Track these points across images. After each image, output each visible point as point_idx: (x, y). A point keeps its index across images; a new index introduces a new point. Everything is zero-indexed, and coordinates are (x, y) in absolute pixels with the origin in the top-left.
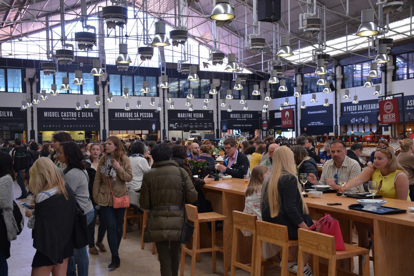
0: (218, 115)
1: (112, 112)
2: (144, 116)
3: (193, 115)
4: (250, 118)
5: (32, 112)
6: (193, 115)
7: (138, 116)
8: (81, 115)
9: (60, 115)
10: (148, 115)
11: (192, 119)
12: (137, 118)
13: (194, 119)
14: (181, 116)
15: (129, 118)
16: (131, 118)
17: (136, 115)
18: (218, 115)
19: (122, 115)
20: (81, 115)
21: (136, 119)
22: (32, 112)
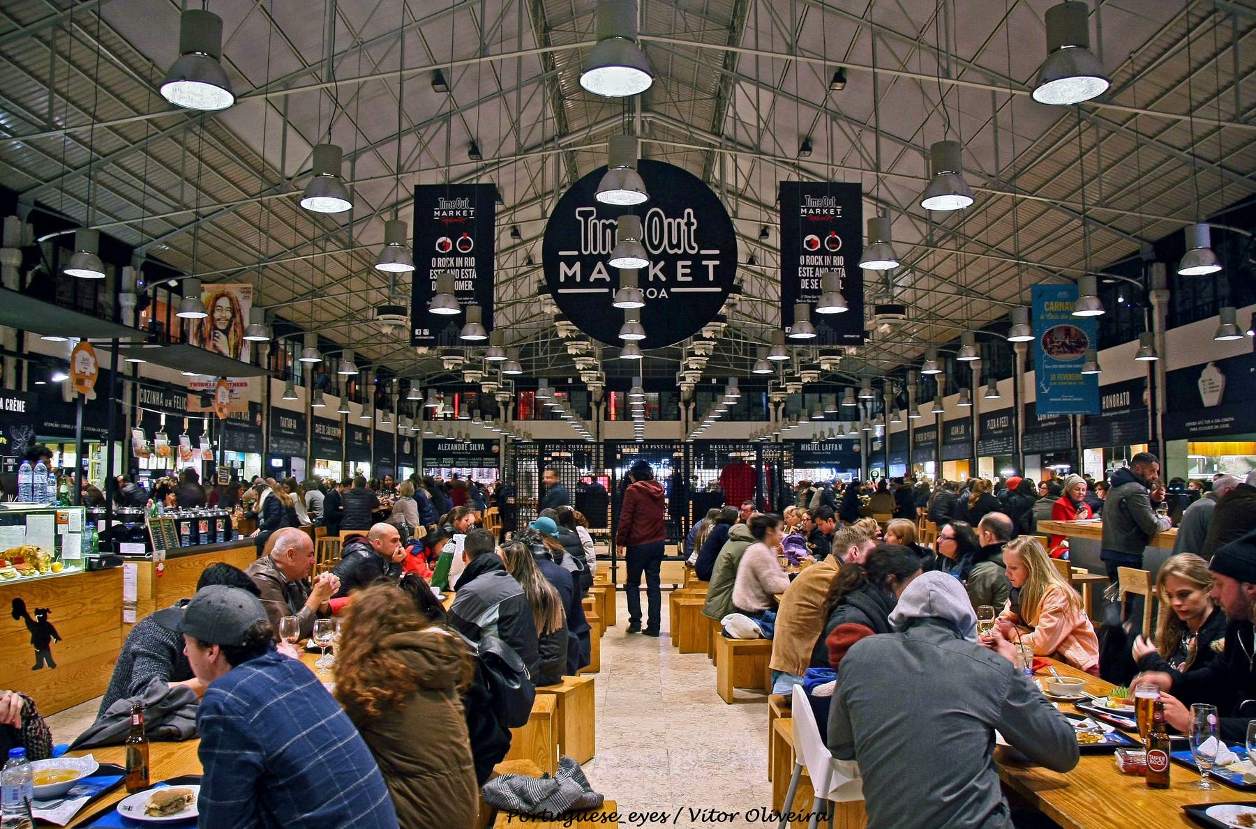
4: (838, 451)
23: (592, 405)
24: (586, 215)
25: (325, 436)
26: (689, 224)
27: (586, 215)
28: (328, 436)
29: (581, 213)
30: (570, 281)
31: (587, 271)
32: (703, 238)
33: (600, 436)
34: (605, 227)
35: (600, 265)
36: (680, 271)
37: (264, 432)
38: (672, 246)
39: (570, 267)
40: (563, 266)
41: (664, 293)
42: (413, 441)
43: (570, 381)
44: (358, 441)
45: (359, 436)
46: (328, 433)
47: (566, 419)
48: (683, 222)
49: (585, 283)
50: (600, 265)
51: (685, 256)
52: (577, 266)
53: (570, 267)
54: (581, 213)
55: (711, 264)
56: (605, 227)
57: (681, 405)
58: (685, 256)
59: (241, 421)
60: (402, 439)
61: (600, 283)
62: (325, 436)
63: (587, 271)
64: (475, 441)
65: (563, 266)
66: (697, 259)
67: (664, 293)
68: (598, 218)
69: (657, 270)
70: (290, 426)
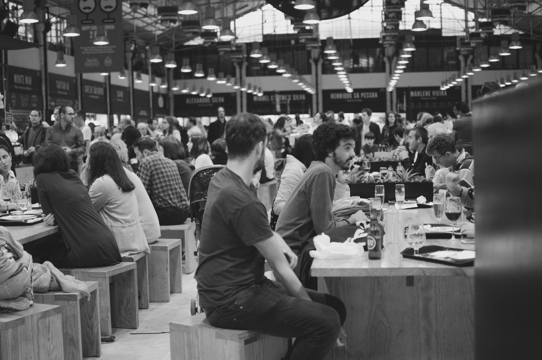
0: (467, 91)
1: (327, 93)
2: (366, 96)
3: (431, 94)
5: (241, 97)
6: (431, 94)
7: (358, 96)
8: (292, 98)
9: (270, 98)
10: (372, 95)
11: (430, 99)
12: (357, 99)
13: (433, 98)
14: (416, 95)
15: (347, 99)
16: (350, 99)
17: (356, 95)
18: (467, 91)
19: (339, 96)
20: (292, 98)
21: (356, 101)
22: (241, 97)
23: (311, 61)
25: (93, 94)
28: (95, 95)
33: (319, 87)
37: (44, 94)
42: (166, 97)
43: (293, 42)
44: (120, 98)
45: (120, 94)
46: (95, 92)
47: (281, 74)
57: (385, 59)
59: (25, 85)
60: (156, 95)
62: (93, 94)
64: (215, 95)
70: (64, 87)
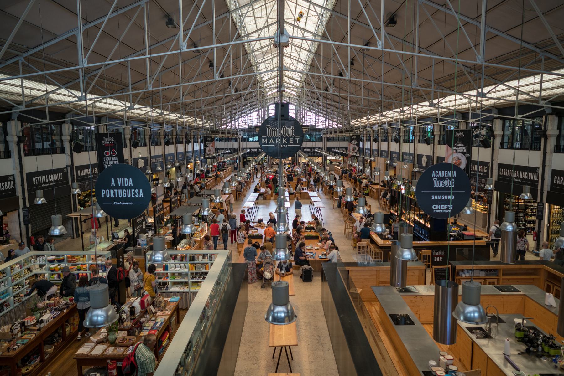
24: (268, 127)
26: (292, 130)
27: (268, 127)
29: (267, 127)
30: (265, 143)
31: (268, 141)
32: (296, 133)
34: (273, 130)
35: (272, 139)
36: (290, 141)
38: (288, 135)
39: (265, 140)
40: (263, 140)
41: (286, 146)
48: (291, 129)
49: (268, 144)
50: (272, 139)
51: (291, 137)
52: (266, 140)
53: (265, 140)
54: (267, 127)
55: (297, 139)
56: (273, 130)
58: (291, 137)
61: (272, 144)
63: (268, 141)
65: (263, 140)
66: (294, 138)
67: (286, 146)
68: (271, 128)
69: (285, 141)
